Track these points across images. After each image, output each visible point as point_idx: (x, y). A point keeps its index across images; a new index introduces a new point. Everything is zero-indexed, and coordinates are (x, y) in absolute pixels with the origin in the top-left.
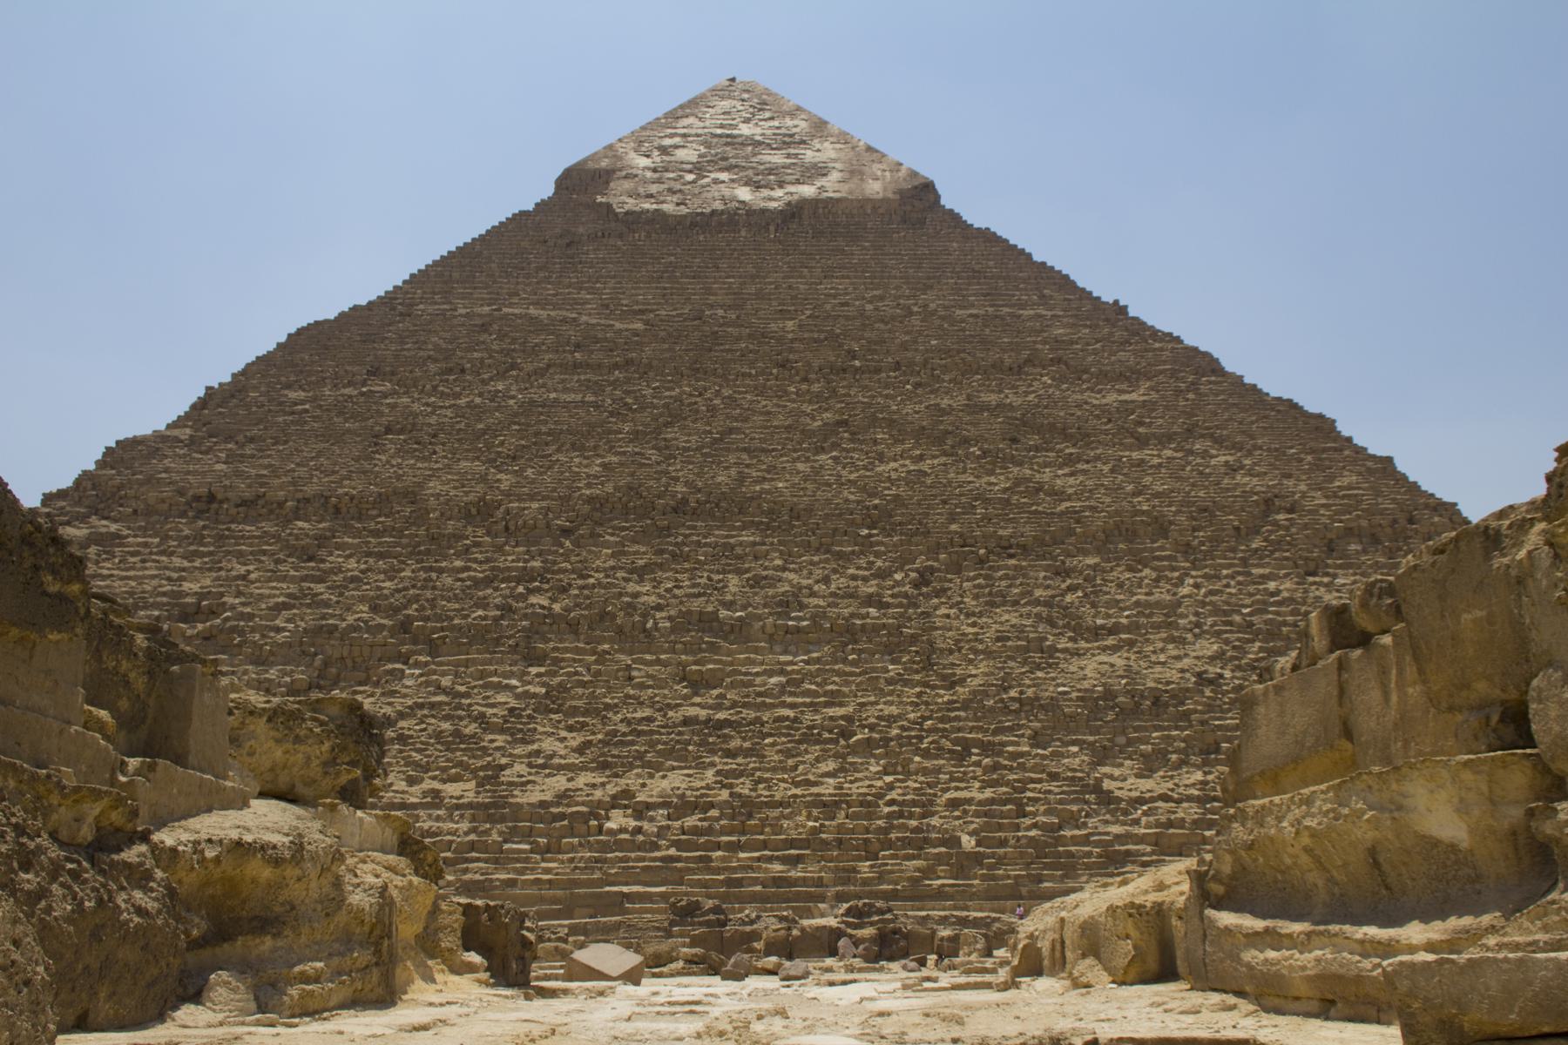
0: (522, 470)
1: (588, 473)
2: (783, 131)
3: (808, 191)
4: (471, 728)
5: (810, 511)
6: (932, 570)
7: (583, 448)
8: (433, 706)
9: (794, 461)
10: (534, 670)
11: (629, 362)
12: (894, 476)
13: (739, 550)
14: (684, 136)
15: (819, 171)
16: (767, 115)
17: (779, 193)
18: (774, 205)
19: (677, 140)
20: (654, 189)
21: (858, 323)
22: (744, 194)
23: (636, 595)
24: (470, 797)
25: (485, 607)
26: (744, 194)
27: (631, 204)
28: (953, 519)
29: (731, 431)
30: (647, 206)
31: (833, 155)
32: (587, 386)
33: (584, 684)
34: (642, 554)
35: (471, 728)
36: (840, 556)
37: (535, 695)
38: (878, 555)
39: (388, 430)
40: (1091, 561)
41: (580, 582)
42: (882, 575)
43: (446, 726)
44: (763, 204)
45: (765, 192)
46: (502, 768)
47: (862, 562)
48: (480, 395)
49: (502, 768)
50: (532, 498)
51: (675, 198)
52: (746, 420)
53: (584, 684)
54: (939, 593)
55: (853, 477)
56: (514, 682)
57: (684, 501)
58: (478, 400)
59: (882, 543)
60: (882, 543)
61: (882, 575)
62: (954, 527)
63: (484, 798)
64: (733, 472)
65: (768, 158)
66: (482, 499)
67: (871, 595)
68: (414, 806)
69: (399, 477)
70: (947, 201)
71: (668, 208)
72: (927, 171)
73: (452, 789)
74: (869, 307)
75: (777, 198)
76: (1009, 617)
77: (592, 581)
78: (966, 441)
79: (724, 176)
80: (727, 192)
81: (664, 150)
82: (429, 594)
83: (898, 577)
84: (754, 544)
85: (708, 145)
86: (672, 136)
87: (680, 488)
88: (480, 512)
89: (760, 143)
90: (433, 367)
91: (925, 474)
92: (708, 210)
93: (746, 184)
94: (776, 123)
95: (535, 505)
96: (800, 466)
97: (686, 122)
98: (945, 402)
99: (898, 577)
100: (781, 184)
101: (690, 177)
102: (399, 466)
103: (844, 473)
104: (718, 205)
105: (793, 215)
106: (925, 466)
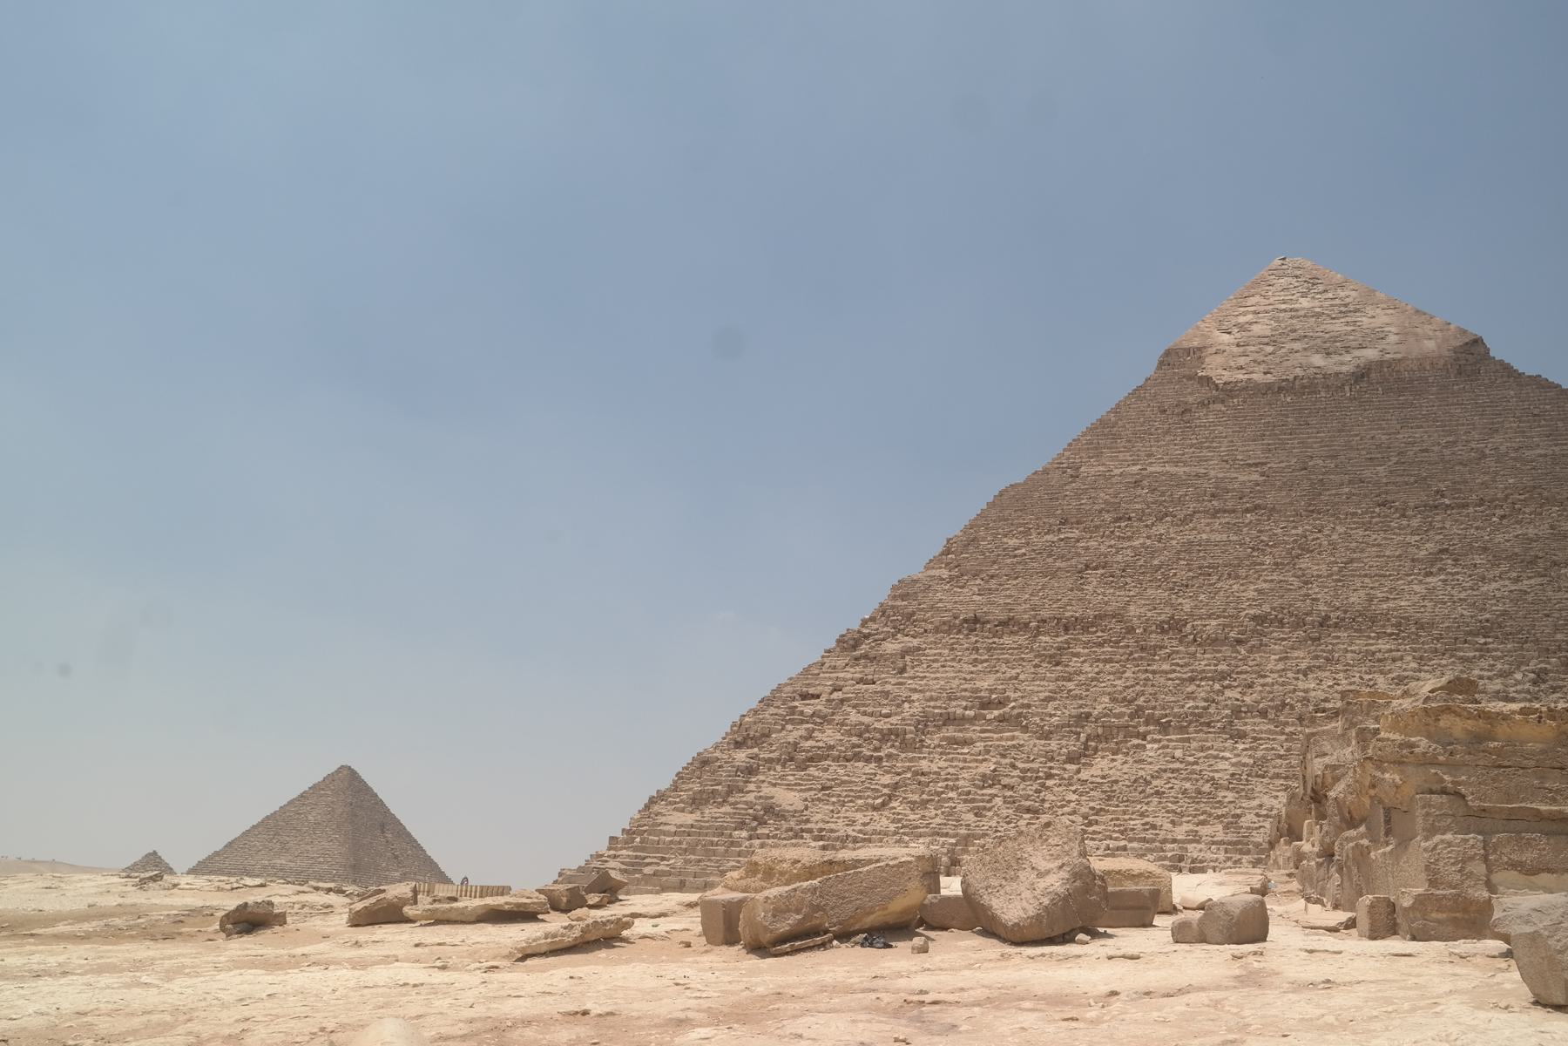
0: (1196, 595)
1: (1248, 594)
2: (1338, 302)
3: (1371, 354)
4: (1207, 788)
5: (1432, 625)
6: (1546, 671)
7: (1237, 577)
8: (1173, 771)
9: (1410, 583)
10: (1241, 746)
11: (1257, 507)
12: (1498, 594)
13: (1379, 656)
14: (1255, 313)
15: (1379, 336)
16: (1321, 288)
17: (1347, 358)
18: (1344, 369)
19: (1250, 317)
20: (1242, 361)
21: (1440, 466)
22: (1318, 360)
23: (1306, 691)
24: (1220, 837)
25: (1194, 699)
26: (1318, 360)
27: (1227, 376)
28: (1557, 629)
29: (1352, 561)
30: (1241, 377)
31: (1386, 319)
32: (1228, 527)
33: (1280, 757)
34: (1302, 658)
35: (1207, 788)
36: (1467, 660)
37: (1245, 765)
38: (1496, 659)
39: (1087, 567)
41: (1262, 681)
42: (1504, 675)
43: (1188, 785)
44: (1337, 369)
45: (1336, 358)
46: (1239, 816)
47: (1484, 664)
48: (1149, 538)
49: (1239, 816)
50: (1210, 617)
51: (1263, 368)
52: (1362, 551)
53: (1280, 757)
54: (1554, 689)
55: (1462, 595)
56: (1227, 755)
57: (1327, 618)
58: (1148, 542)
59: (1496, 650)
60: (1496, 650)
61: (1504, 675)
62: (1559, 636)
63: (1231, 837)
64: (1362, 593)
65: (1330, 328)
66: (1172, 618)
67: (1498, 692)
68: (1183, 842)
69: (1106, 603)
70: (1497, 352)
71: (1258, 377)
72: (1476, 330)
73: (1204, 831)
74: (1447, 452)
75: (1346, 363)
77: (1269, 680)
78: (1555, 563)
79: (1297, 346)
80: (1304, 361)
81: (1242, 328)
82: (1150, 690)
83: (1518, 676)
84: (1391, 651)
85: (1277, 320)
86: (1244, 314)
87: (1322, 607)
88: (1173, 626)
89: (1318, 315)
90: (1108, 517)
91: (1526, 593)
92: (1291, 378)
93: (1317, 352)
94: (1330, 295)
95: (1214, 623)
96: (1417, 588)
97: (1252, 301)
98: (1531, 531)
99: (1518, 676)
100: (1347, 350)
101: (1270, 349)
102: (1104, 594)
103: (1454, 592)
104: (1299, 372)
105: (1363, 376)
106: (1525, 584)
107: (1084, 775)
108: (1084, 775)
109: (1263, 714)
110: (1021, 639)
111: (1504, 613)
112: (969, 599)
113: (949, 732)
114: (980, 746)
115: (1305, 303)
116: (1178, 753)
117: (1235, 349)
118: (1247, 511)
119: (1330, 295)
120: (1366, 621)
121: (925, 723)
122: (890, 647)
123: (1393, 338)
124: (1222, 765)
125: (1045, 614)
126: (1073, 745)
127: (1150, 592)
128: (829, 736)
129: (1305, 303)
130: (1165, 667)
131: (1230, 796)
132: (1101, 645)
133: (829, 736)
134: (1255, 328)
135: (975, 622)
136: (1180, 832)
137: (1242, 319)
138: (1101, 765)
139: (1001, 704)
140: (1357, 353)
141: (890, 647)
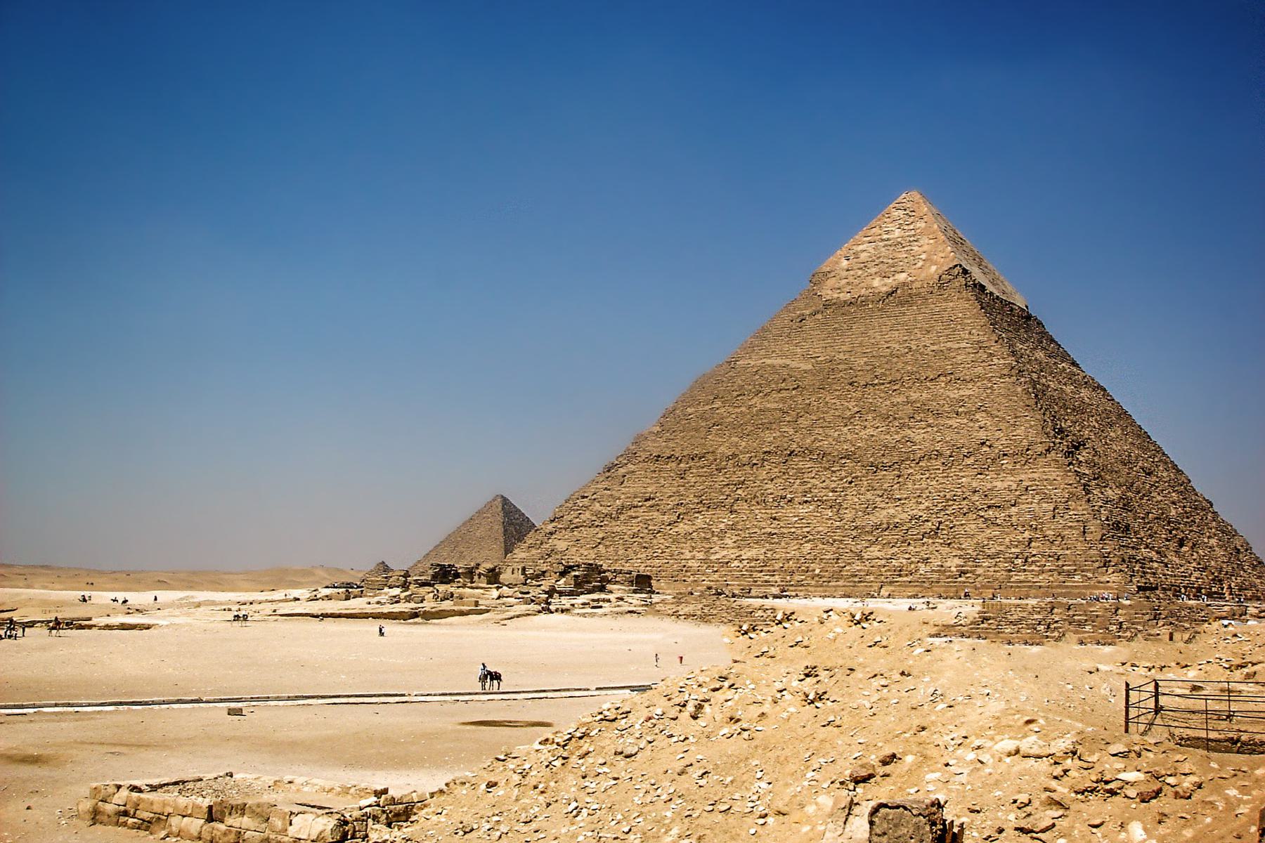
16: (911, 220)
17: (890, 280)
18: (884, 289)
22: (876, 282)
101: (860, 272)
104: (863, 292)
110: (674, 465)
112: (654, 447)
113: (631, 513)
115: (897, 233)
117: (845, 274)
121: (621, 510)
122: (622, 471)
125: (685, 453)
133: (587, 515)
137: (861, 247)
141: (622, 471)
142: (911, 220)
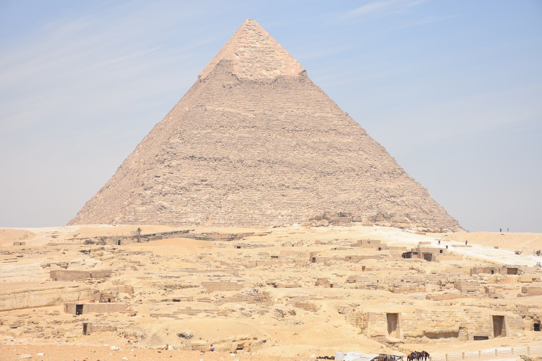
2: (267, 46)
3: (278, 72)
17: (272, 73)
18: (272, 78)
20: (244, 69)
26: (264, 72)
32: (248, 132)
40: (342, 177)
71: (249, 77)
75: (271, 75)
76: (330, 187)
79: (258, 65)
86: (241, 47)
89: (263, 51)
93: (264, 69)
94: (265, 42)
107: (228, 199)
108: (228, 199)
109: (263, 185)
111: (309, 163)
114: (203, 191)
116: (247, 194)
118: (253, 127)
119: (265, 42)
120: (281, 162)
123: (283, 66)
124: (256, 197)
126: (224, 192)
127: (233, 151)
128: (167, 188)
129: (258, 45)
130: (240, 173)
131: (259, 204)
132: (224, 166)
134: (245, 54)
135: (193, 157)
136: (251, 212)
138: (230, 197)
139: (206, 181)
140: (275, 71)
142: (262, 38)
